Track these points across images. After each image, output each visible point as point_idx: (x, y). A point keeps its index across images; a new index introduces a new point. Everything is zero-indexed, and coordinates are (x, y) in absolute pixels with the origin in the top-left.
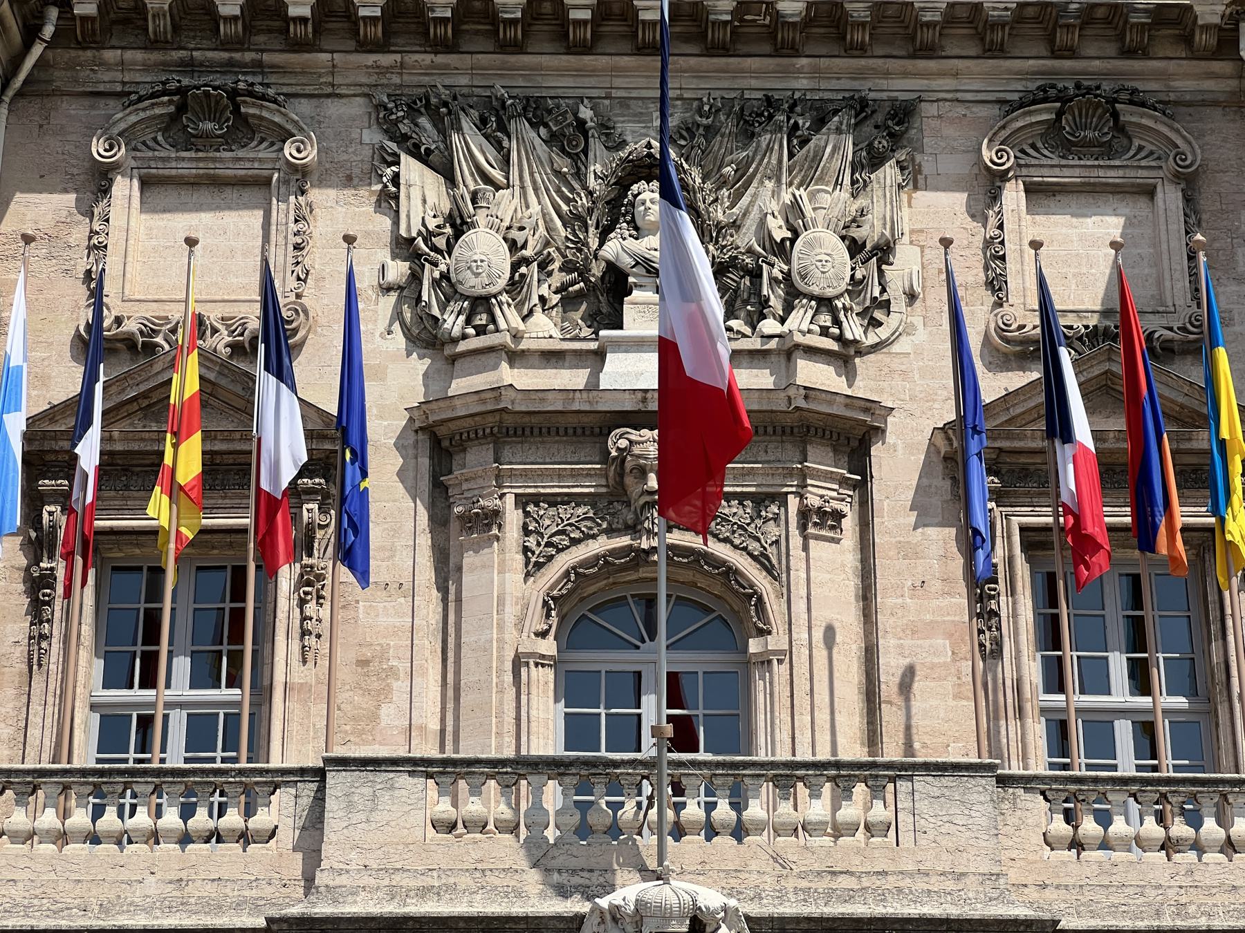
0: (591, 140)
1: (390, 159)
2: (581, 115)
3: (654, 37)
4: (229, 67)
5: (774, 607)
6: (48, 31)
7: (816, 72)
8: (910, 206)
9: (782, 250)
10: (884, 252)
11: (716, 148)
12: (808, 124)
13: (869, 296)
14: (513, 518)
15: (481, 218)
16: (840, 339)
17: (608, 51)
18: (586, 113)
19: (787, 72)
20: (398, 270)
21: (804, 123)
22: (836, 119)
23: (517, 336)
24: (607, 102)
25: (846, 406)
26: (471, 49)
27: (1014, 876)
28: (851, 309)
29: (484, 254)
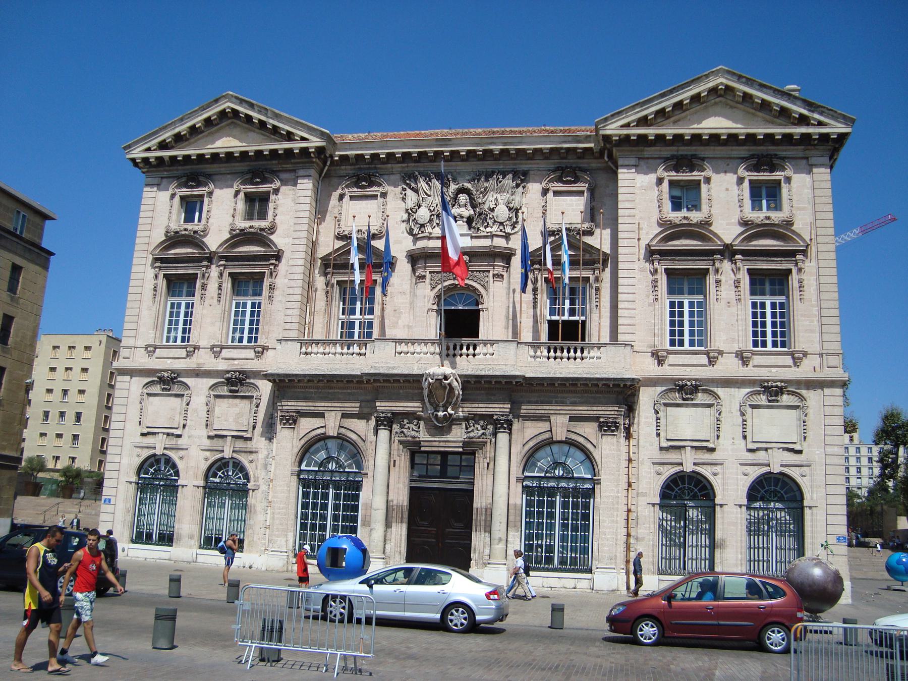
4: (369, 168)
5: (485, 297)
6: (329, 163)
7: (504, 164)
9: (493, 210)
10: (517, 210)
14: (428, 276)
15: (423, 205)
19: (499, 164)
20: (405, 216)
21: (501, 177)
23: (430, 233)
27: (520, 364)
29: (423, 214)
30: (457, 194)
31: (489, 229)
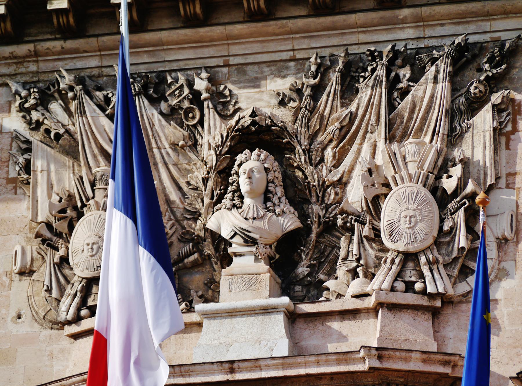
0: (206, 111)
1: (24, 146)
2: (196, 87)
3: (259, 5)
7: (419, 21)
8: (508, 148)
9: (375, 204)
11: (322, 108)
12: (408, 76)
13: (456, 246)
16: (424, 292)
17: (222, 21)
18: (201, 85)
21: (405, 73)
22: (434, 67)
24: (225, 70)
25: (424, 361)
26: (97, 32)
28: (437, 261)
30: (233, 152)
31: (356, 286)
